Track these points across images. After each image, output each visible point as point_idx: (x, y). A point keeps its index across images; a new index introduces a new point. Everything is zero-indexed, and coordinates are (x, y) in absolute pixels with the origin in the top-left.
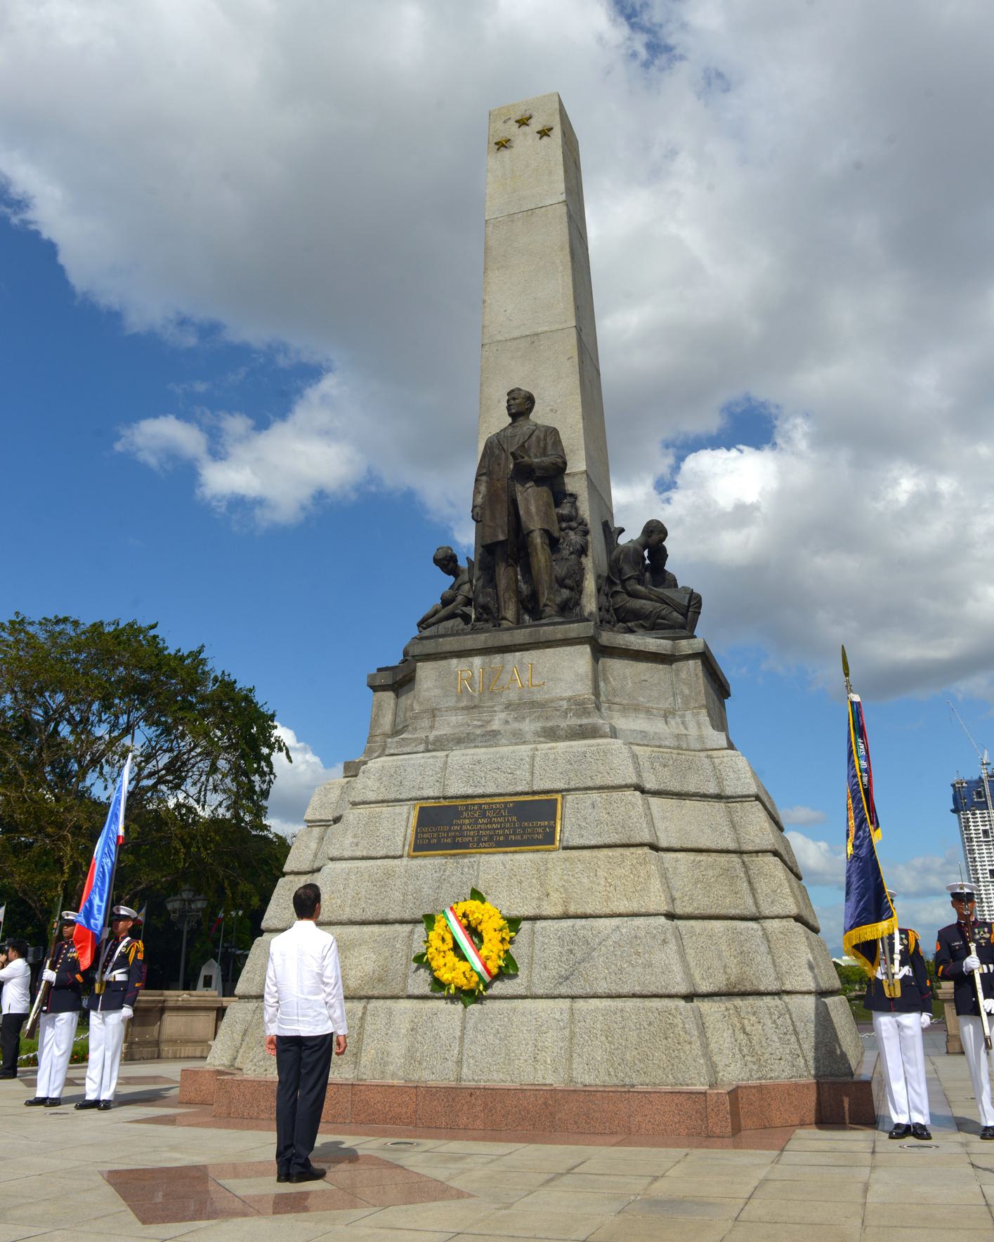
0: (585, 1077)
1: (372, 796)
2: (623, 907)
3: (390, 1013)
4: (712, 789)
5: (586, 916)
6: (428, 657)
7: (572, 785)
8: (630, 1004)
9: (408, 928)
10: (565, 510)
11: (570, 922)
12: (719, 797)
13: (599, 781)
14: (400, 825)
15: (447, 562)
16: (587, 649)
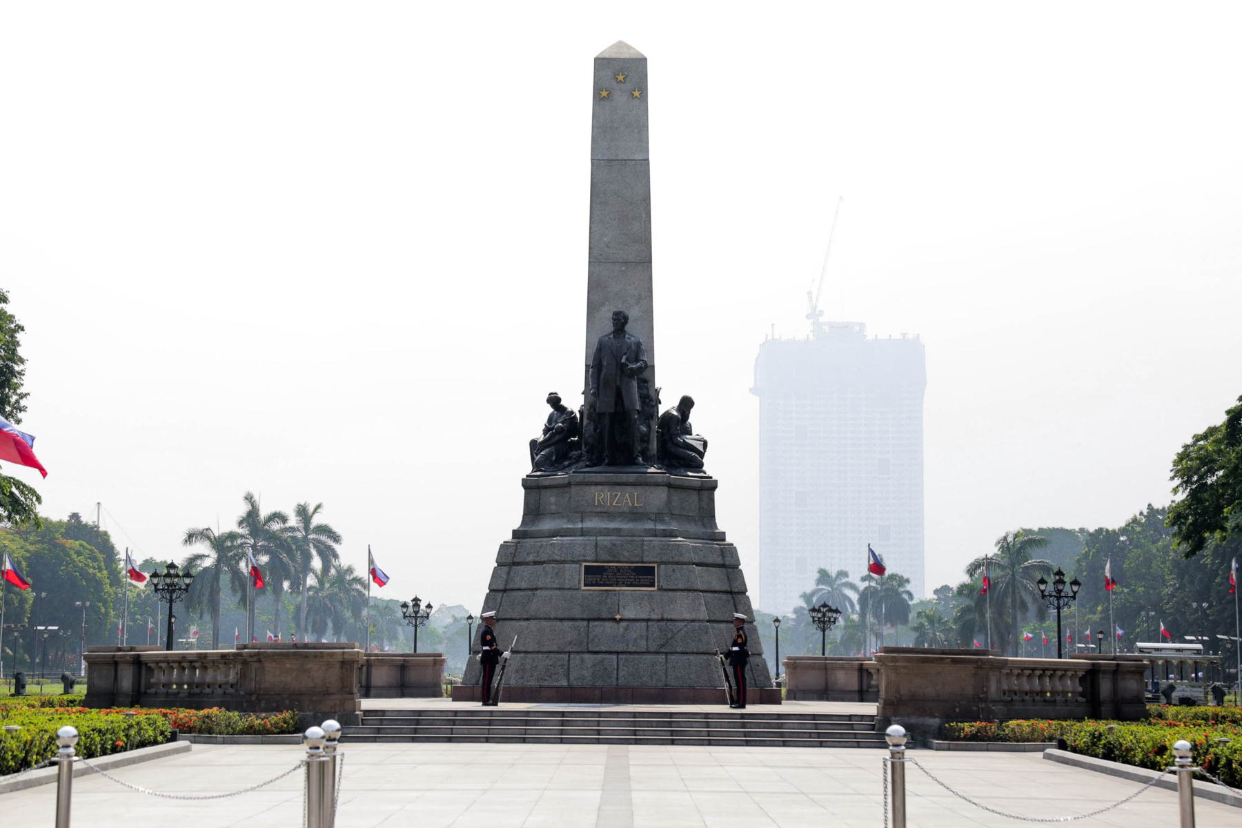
0: (672, 682)
1: (558, 558)
2: (688, 616)
3: (582, 660)
4: (719, 561)
5: (671, 620)
6: (579, 484)
7: (664, 559)
8: (691, 657)
9: (585, 623)
10: (645, 392)
11: (663, 623)
12: (723, 566)
13: (676, 559)
14: (575, 574)
15: (554, 401)
16: (666, 489)
